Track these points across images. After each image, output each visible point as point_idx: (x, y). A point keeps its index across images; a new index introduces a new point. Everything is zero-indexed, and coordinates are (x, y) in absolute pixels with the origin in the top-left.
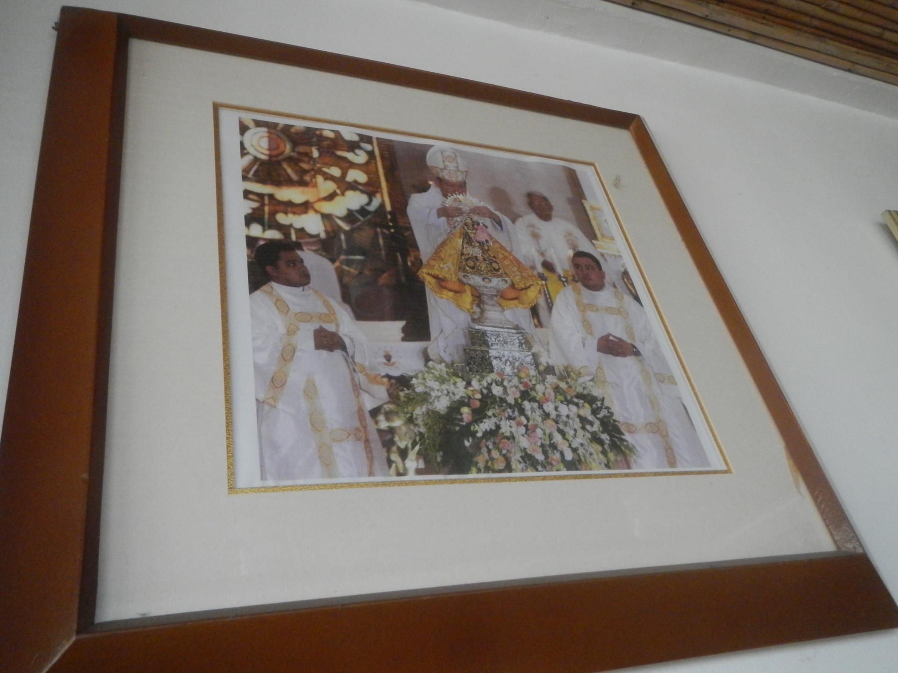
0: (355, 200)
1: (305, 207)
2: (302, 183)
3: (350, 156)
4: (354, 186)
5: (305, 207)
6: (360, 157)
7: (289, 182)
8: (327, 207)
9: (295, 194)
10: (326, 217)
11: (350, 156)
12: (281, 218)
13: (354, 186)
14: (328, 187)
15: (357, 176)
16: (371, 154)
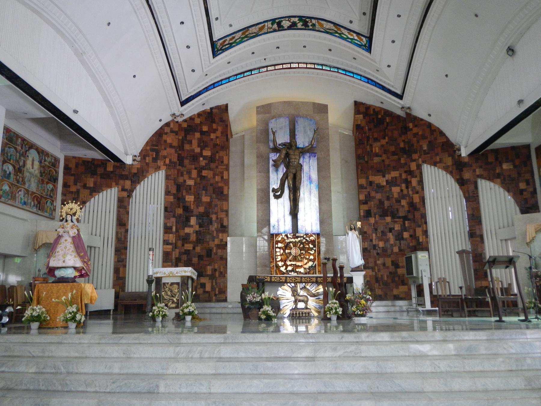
0: (310, 264)
1: (301, 266)
2: (301, 261)
3: (311, 252)
4: (311, 260)
5: (301, 266)
6: (312, 252)
7: (299, 261)
8: (305, 266)
10: (305, 268)
11: (311, 252)
12: (297, 270)
13: (311, 260)
14: (306, 261)
15: (312, 257)
16: (315, 250)
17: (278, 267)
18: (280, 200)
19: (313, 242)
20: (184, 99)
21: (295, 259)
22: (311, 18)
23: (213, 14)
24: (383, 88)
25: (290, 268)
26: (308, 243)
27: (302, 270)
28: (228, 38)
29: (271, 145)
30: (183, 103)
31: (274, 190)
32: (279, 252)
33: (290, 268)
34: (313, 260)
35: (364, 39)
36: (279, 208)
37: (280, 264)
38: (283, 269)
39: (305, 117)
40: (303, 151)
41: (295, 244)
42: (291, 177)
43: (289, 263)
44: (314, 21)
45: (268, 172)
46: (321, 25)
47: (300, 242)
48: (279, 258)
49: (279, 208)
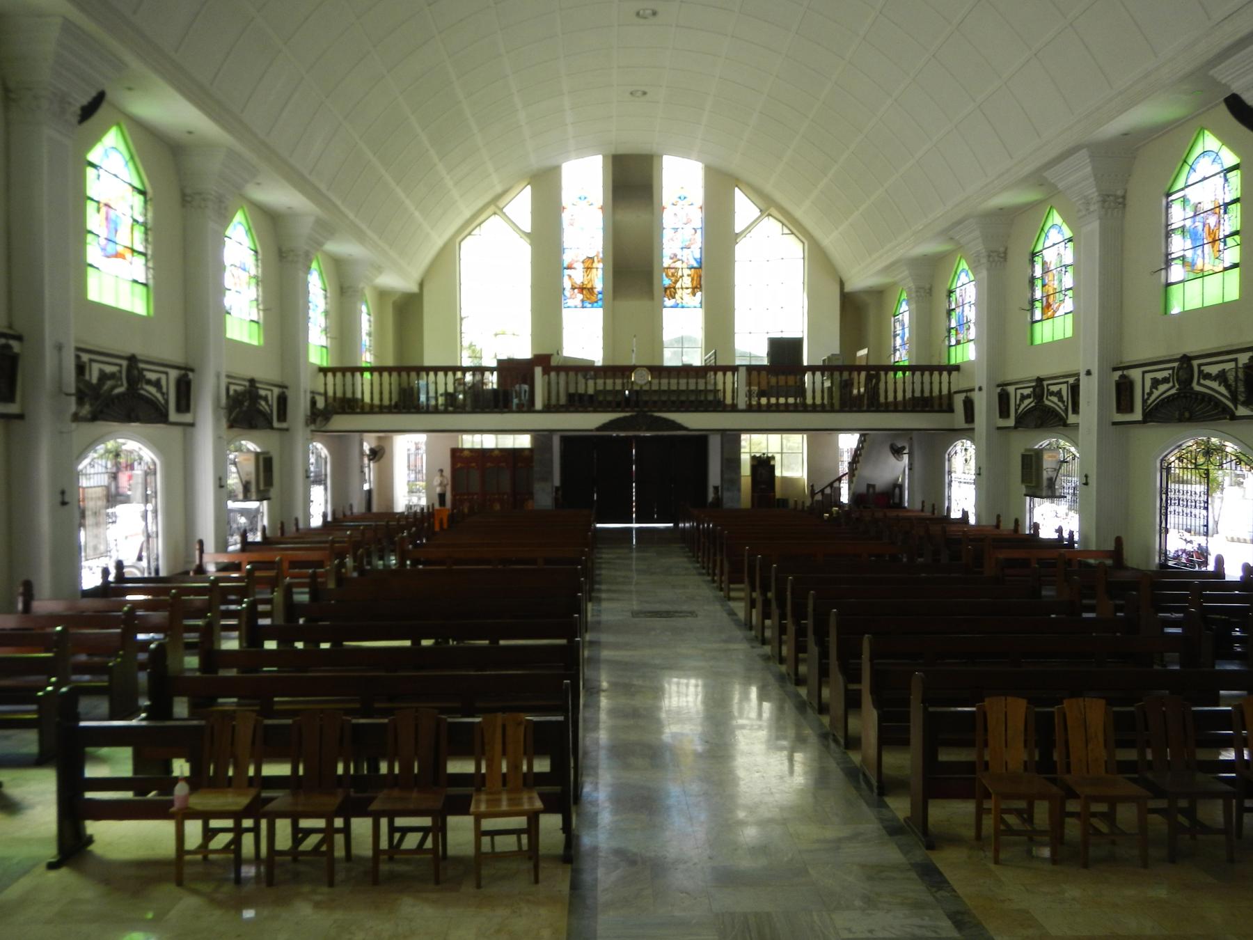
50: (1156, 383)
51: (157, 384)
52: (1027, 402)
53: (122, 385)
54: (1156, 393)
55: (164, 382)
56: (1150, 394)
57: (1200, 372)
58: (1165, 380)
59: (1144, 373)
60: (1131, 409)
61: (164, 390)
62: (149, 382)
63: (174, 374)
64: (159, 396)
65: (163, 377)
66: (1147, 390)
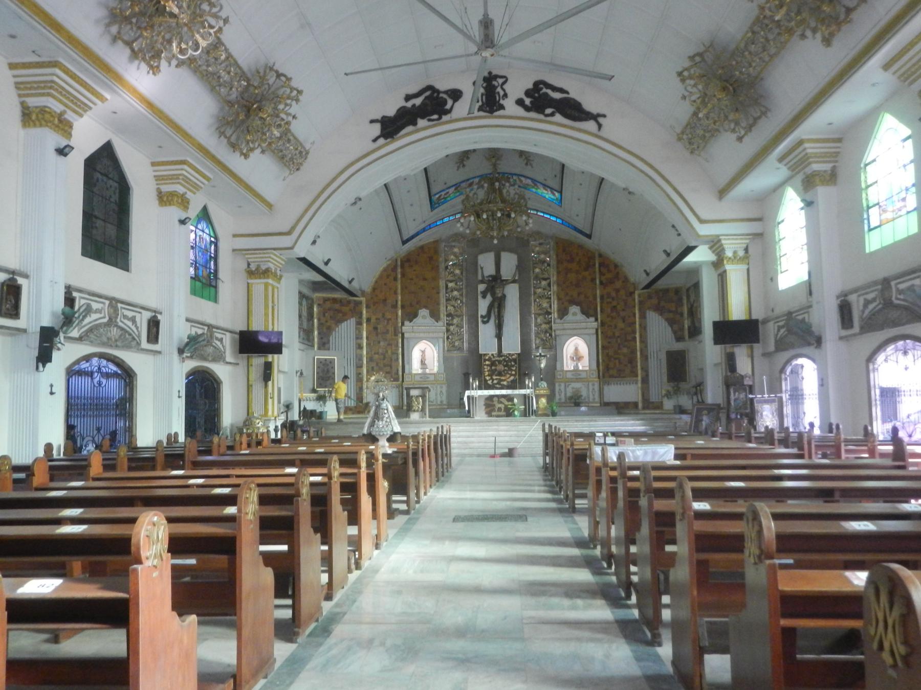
0: (512, 378)
9: (503, 378)
13: (511, 375)
17: (486, 381)
18: (487, 325)
19: (515, 360)
20: (405, 238)
21: (500, 374)
22: (512, 174)
23: (431, 180)
24: (576, 229)
25: (495, 382)
26: (511, 361)
27: (505, 383)
28: (443, 193)
29: (480, 278)
30: (404, 242)
31: (482, 316)
32: (486, 369)
33: (495, 382)
34: (515, 375)
35: (557, 194)
36: (486, 332)
37: (488, 378)
38: (490, 382)
39: (511, 251)
40: (505, 282)
41: (500, 362)
42: (496, 304)
43: (494, 377)
44: (515, 177)
45: (477, 300)
46: (521, 181)
47: (504, 360)
48: (487, 373)
49: (486, 332)
50: (867, 303)
51: (133, 320)
52: (782, 331)
53: (104, 317)
54: (867, 312)
55: (138, 320)
56: (863, 312)
57: (898, 290)
58: (874, 300)
59: (859, 296)
60: (852, 327)
61: (138, 325)
62: (125, 317)
63: (147, 315)
64: (134, 329)
65: (138, 315)
66: (861, 308)
